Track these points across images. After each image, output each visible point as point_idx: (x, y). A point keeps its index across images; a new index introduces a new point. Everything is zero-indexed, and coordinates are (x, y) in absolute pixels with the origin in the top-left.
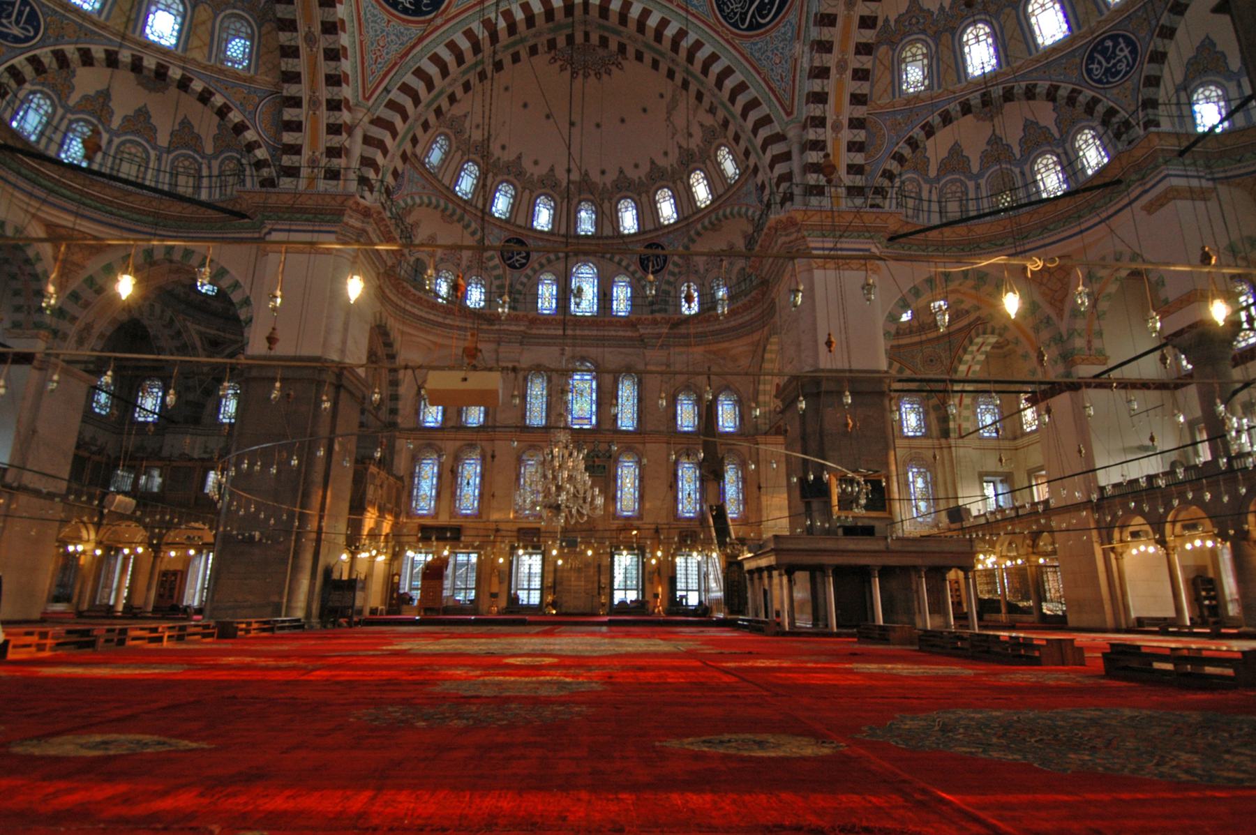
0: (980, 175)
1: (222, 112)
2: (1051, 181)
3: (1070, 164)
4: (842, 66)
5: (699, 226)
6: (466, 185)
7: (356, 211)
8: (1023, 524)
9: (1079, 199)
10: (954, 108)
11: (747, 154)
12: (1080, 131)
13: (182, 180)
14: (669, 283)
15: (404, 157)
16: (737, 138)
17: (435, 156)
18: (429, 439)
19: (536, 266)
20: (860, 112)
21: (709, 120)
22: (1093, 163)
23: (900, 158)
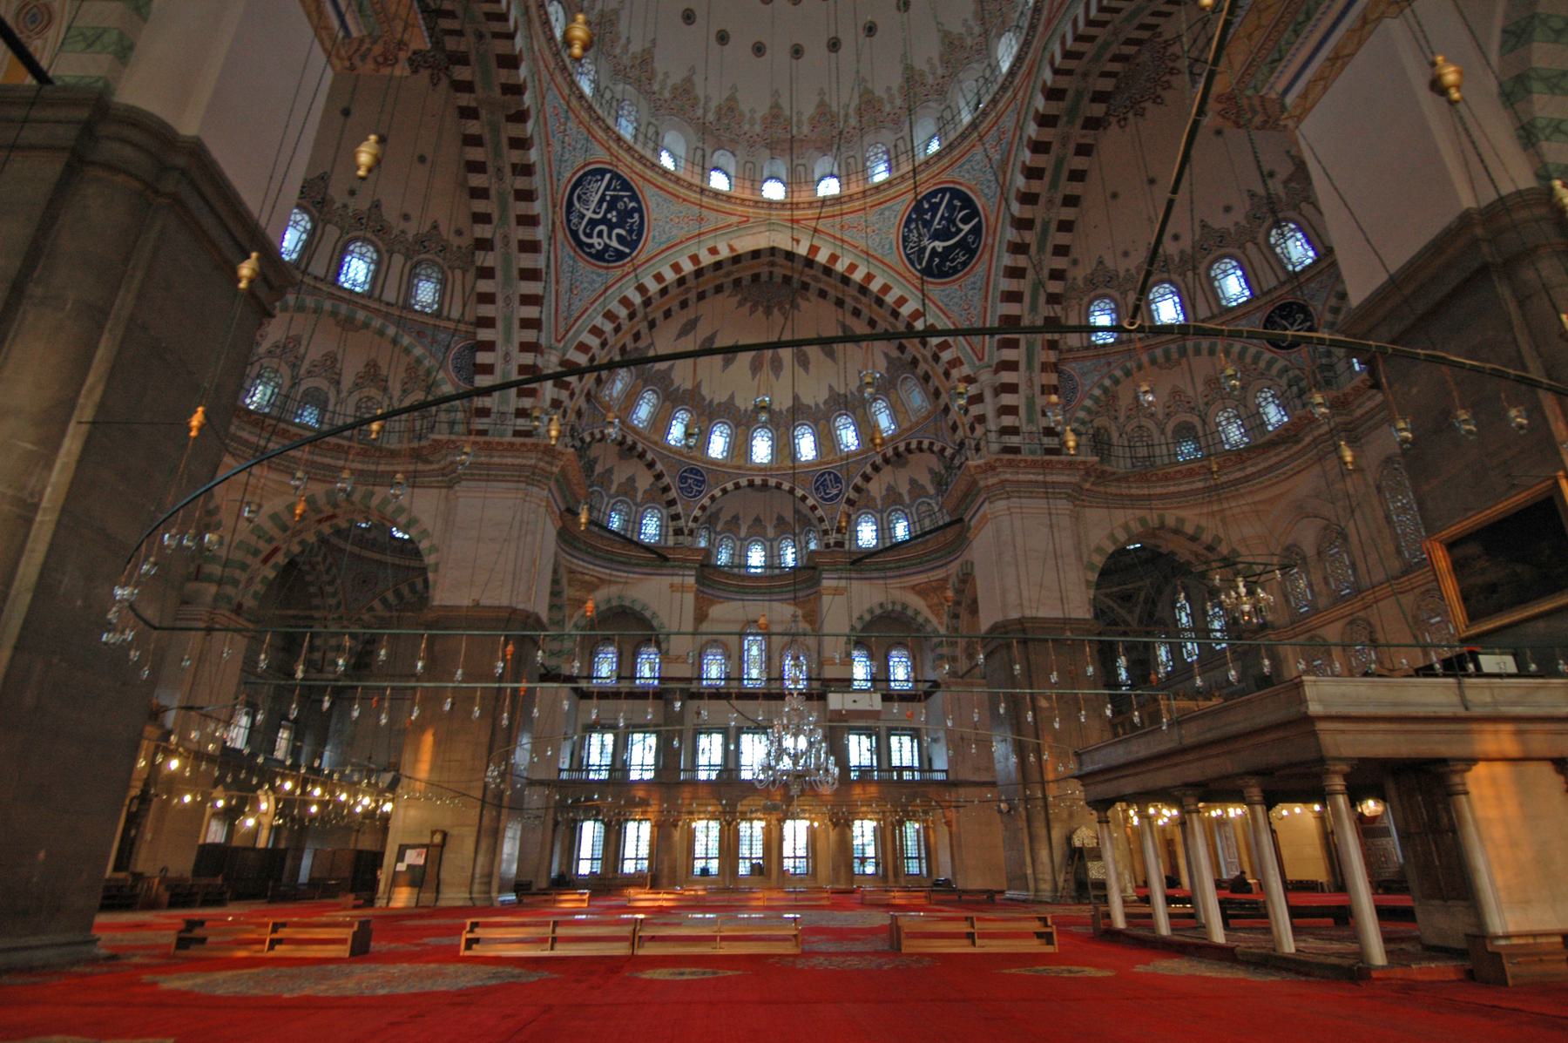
7: (985, 472)
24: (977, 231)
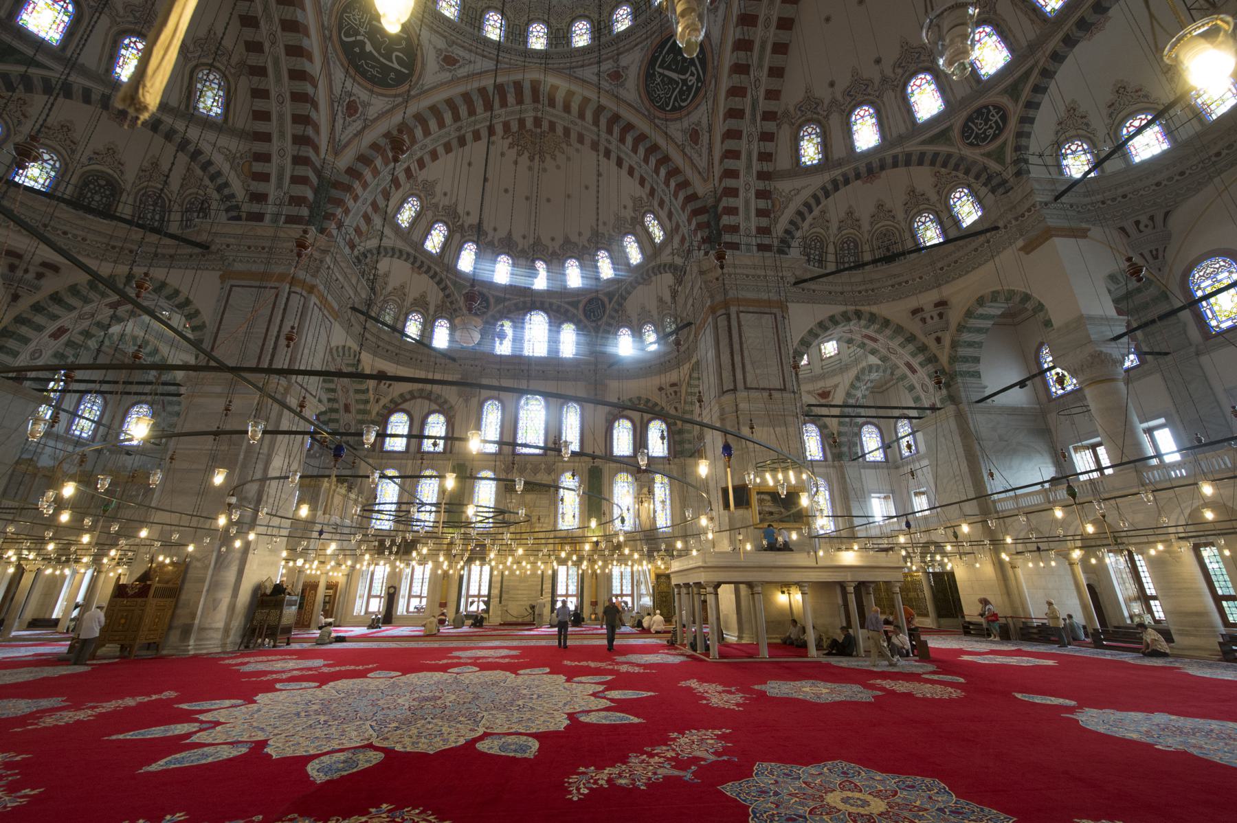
17: (405, 217)
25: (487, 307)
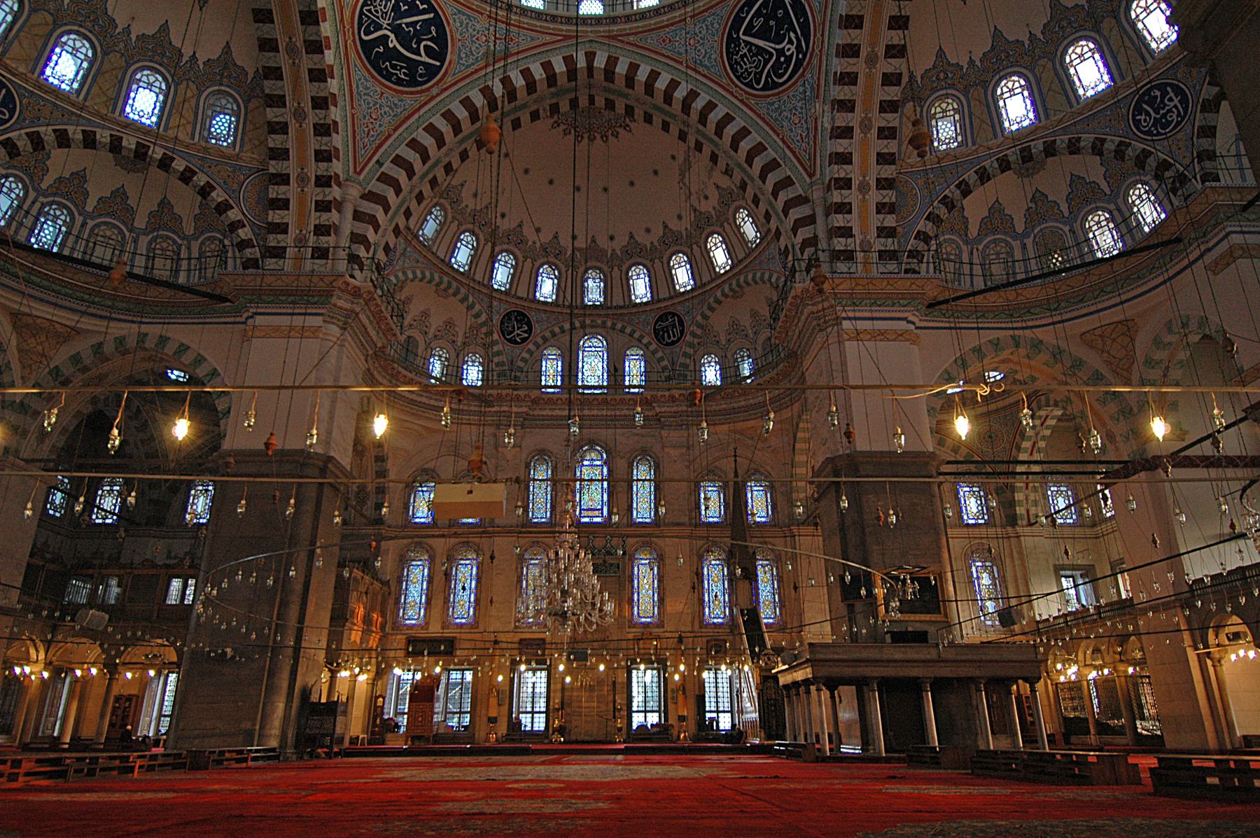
0: (1025, 235)
1: (205, 191)
2: (1105, 240)
3: (1124, 221)
4: (866, 125)
5: (719, 294)
6: (462, 256)
8: (1107, 625)
9: (1134, 260)
10: (990, 164)
11: (768, 216)
12: (1133, 185)
13: (159, 263)
14: (686, 355)
15: (397, 231)
16: (756, 201)
17: (430, 228)
18: (418, 537)
19: (540, 341)
20: (888, 171)
21: (724, 182)
22: (1149, 220)
23: (933, 218)
24: (432, 72)
25: (529, 331)
